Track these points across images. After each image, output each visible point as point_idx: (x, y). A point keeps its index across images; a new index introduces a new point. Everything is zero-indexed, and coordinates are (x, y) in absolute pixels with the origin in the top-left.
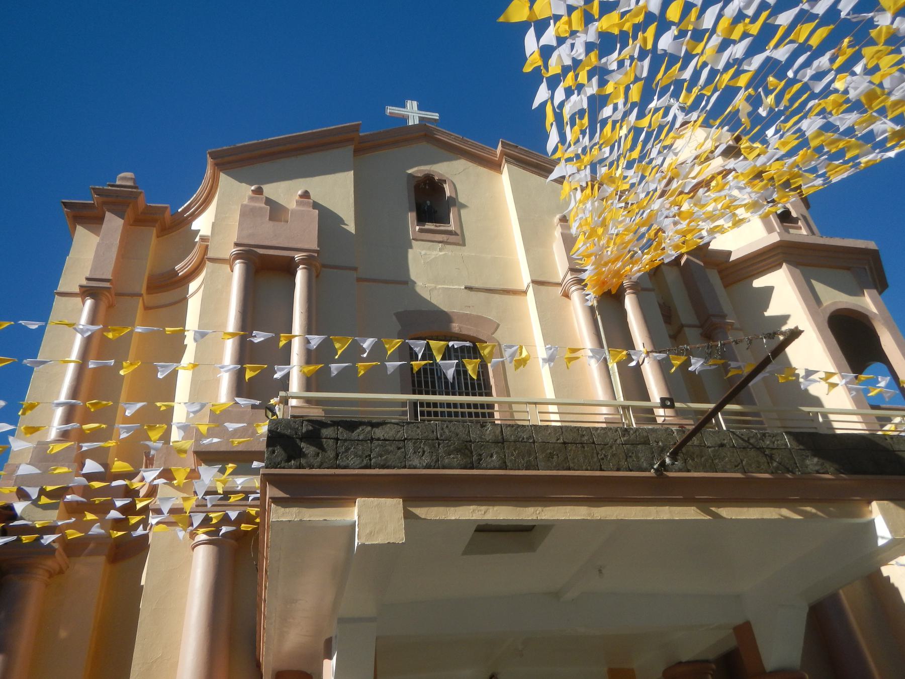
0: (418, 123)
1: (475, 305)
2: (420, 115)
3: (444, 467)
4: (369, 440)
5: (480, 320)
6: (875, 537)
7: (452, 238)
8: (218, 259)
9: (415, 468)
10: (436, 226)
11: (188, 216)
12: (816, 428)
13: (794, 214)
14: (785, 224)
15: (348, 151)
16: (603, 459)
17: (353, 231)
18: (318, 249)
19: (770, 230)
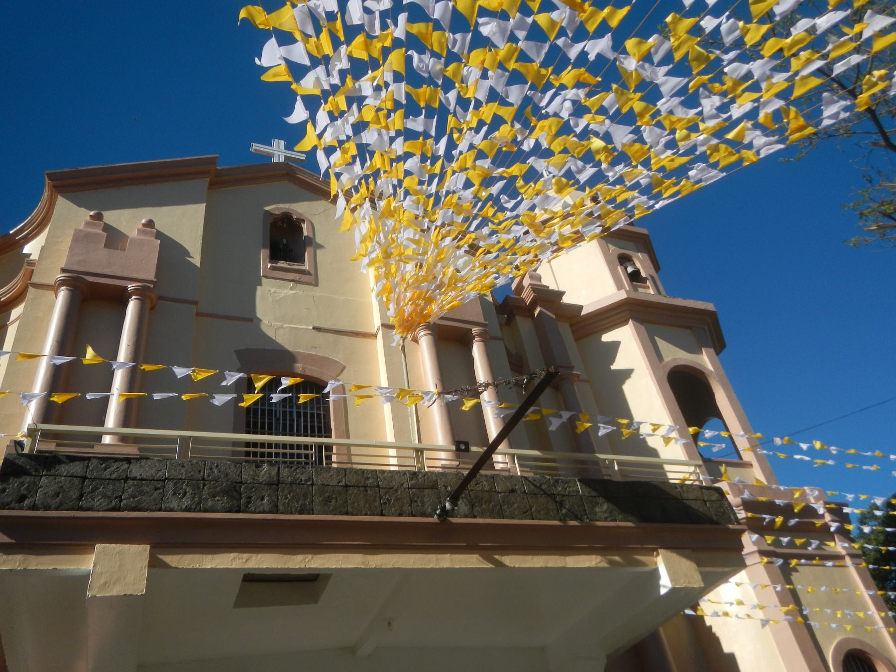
0: (283, 161)
1: (323, 346)
2: (286, 154)
3: (206, 511)
4: (122, 479)
5: (325, 361)
6: (658, 587)
7: (305, 278)
8: (41, 285)
9: (172, 510)
10: (289, 265)
11: (21, 239)
12: (610, 475)
13: (643, 274)
14: (634, 283)
15: (203, 184)
16: (385, 503)
17: (198, 264)
18: (155, 280)
19: (620, 286)
